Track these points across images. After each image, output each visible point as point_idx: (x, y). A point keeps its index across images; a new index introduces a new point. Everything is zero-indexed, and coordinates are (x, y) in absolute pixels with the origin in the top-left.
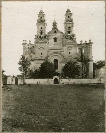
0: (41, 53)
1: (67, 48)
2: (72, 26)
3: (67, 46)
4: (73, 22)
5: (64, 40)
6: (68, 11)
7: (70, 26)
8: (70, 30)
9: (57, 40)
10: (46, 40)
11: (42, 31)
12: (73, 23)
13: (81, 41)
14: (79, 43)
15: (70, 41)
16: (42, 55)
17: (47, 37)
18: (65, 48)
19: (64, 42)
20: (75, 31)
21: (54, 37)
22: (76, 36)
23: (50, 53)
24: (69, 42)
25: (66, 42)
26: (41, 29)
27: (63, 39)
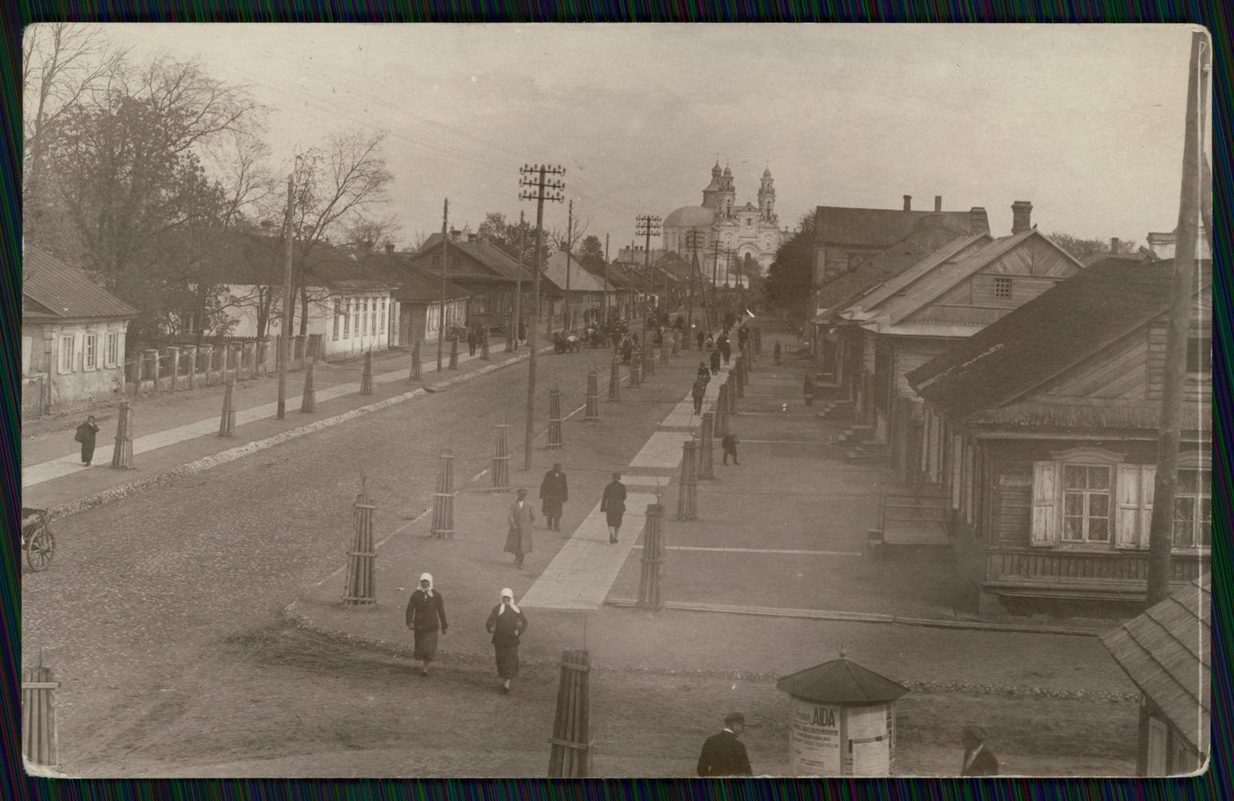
2: (774, 201)
3: (766, 233)
4: (776, 193)
5: (762, 223)
6: (767, 174)
7: (770, 200)
9: (752, 221)
10: (736, 221)
12: (774, 196)
13: (787, 227)
14: (783, 230)
15: (768, 225)
18: (762, 236)
20: (776, 209)
21: (748, 217)
22: (779, 218)
23: (740, 243)
24: (768, 228)
25: (765, 228)
27: (760, 221)
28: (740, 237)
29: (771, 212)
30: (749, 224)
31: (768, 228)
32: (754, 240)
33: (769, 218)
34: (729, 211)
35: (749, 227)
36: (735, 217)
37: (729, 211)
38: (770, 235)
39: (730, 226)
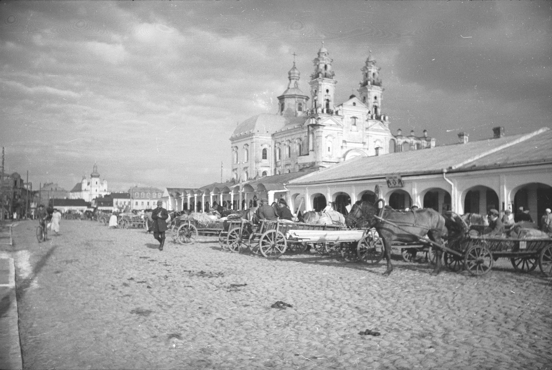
0: (329, 148)
1: (375, 142)
5: (371, 123)
8: (376, 104)
10: (337, 118)
11: (329, 99)
16: (330, 153)
17: (339, 113)
19: (370, 129)
23: (345, 150)
26: (326, 93)
27: (367, 121)
28: (344, 142)
29: (379, 111)
30: (355, 125)
31: (377, 130)
32: (361, 145)
33: (378, 118)
34: (327, 105)
35: (354, 128)
36: (337, 112)
37: (327, 105)
38: (379, 140)
39: (331, 125)
